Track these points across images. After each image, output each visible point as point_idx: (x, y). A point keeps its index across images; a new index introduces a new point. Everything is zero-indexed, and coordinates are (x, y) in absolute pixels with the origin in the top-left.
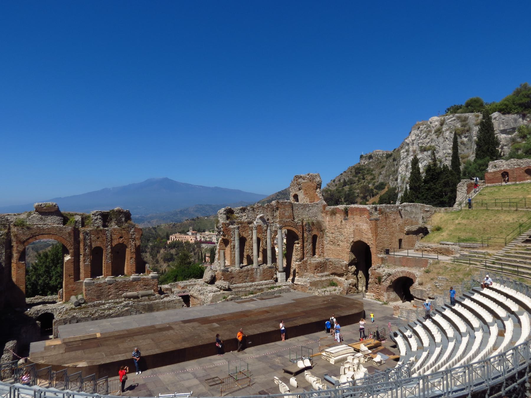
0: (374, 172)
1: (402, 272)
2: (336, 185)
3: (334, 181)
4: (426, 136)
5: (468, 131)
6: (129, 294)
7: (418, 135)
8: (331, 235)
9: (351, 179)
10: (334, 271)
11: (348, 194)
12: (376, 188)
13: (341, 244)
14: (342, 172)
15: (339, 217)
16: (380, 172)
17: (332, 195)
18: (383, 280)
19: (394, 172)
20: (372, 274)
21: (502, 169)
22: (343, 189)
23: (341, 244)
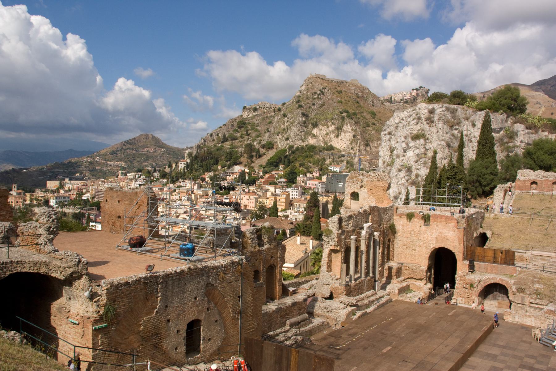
0: (258, 128)
1: (492, 279)
2: (214, 140)
3: (211, 135)
4: (417, 123)
5: (457, 124)
6: (293, 320)
7: (403, 119)
8: (405, 239)
9: (232, 134)
10: (410, 276)
11: (230, 152)
12: (263, 146)
13: (418, 249)
14: (221, 125)
15: (417, 223)
16: (268, 129)
17: (210, 153)
18: (474, 286)
19: (284, 129)
20: (461, 280)
21: (531, 178)
22: (223, 146)
23: (418, 249)
